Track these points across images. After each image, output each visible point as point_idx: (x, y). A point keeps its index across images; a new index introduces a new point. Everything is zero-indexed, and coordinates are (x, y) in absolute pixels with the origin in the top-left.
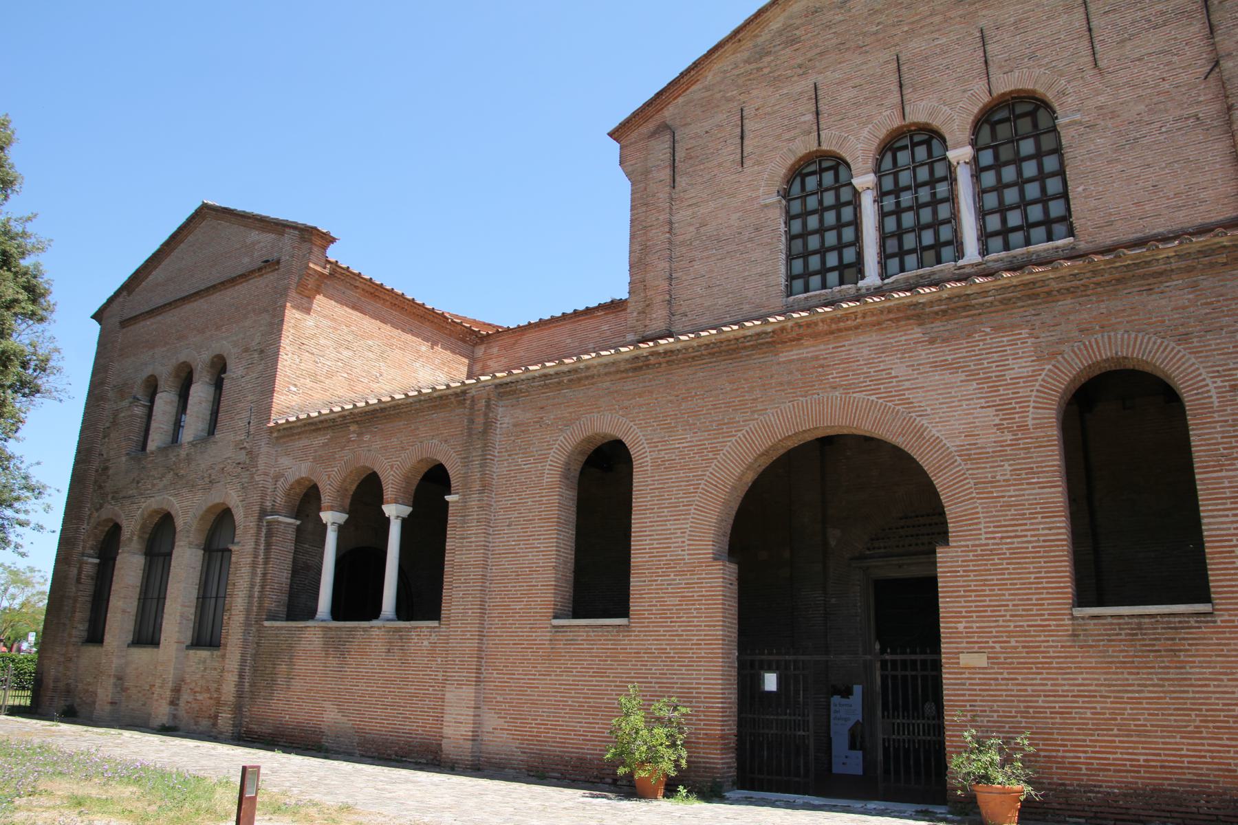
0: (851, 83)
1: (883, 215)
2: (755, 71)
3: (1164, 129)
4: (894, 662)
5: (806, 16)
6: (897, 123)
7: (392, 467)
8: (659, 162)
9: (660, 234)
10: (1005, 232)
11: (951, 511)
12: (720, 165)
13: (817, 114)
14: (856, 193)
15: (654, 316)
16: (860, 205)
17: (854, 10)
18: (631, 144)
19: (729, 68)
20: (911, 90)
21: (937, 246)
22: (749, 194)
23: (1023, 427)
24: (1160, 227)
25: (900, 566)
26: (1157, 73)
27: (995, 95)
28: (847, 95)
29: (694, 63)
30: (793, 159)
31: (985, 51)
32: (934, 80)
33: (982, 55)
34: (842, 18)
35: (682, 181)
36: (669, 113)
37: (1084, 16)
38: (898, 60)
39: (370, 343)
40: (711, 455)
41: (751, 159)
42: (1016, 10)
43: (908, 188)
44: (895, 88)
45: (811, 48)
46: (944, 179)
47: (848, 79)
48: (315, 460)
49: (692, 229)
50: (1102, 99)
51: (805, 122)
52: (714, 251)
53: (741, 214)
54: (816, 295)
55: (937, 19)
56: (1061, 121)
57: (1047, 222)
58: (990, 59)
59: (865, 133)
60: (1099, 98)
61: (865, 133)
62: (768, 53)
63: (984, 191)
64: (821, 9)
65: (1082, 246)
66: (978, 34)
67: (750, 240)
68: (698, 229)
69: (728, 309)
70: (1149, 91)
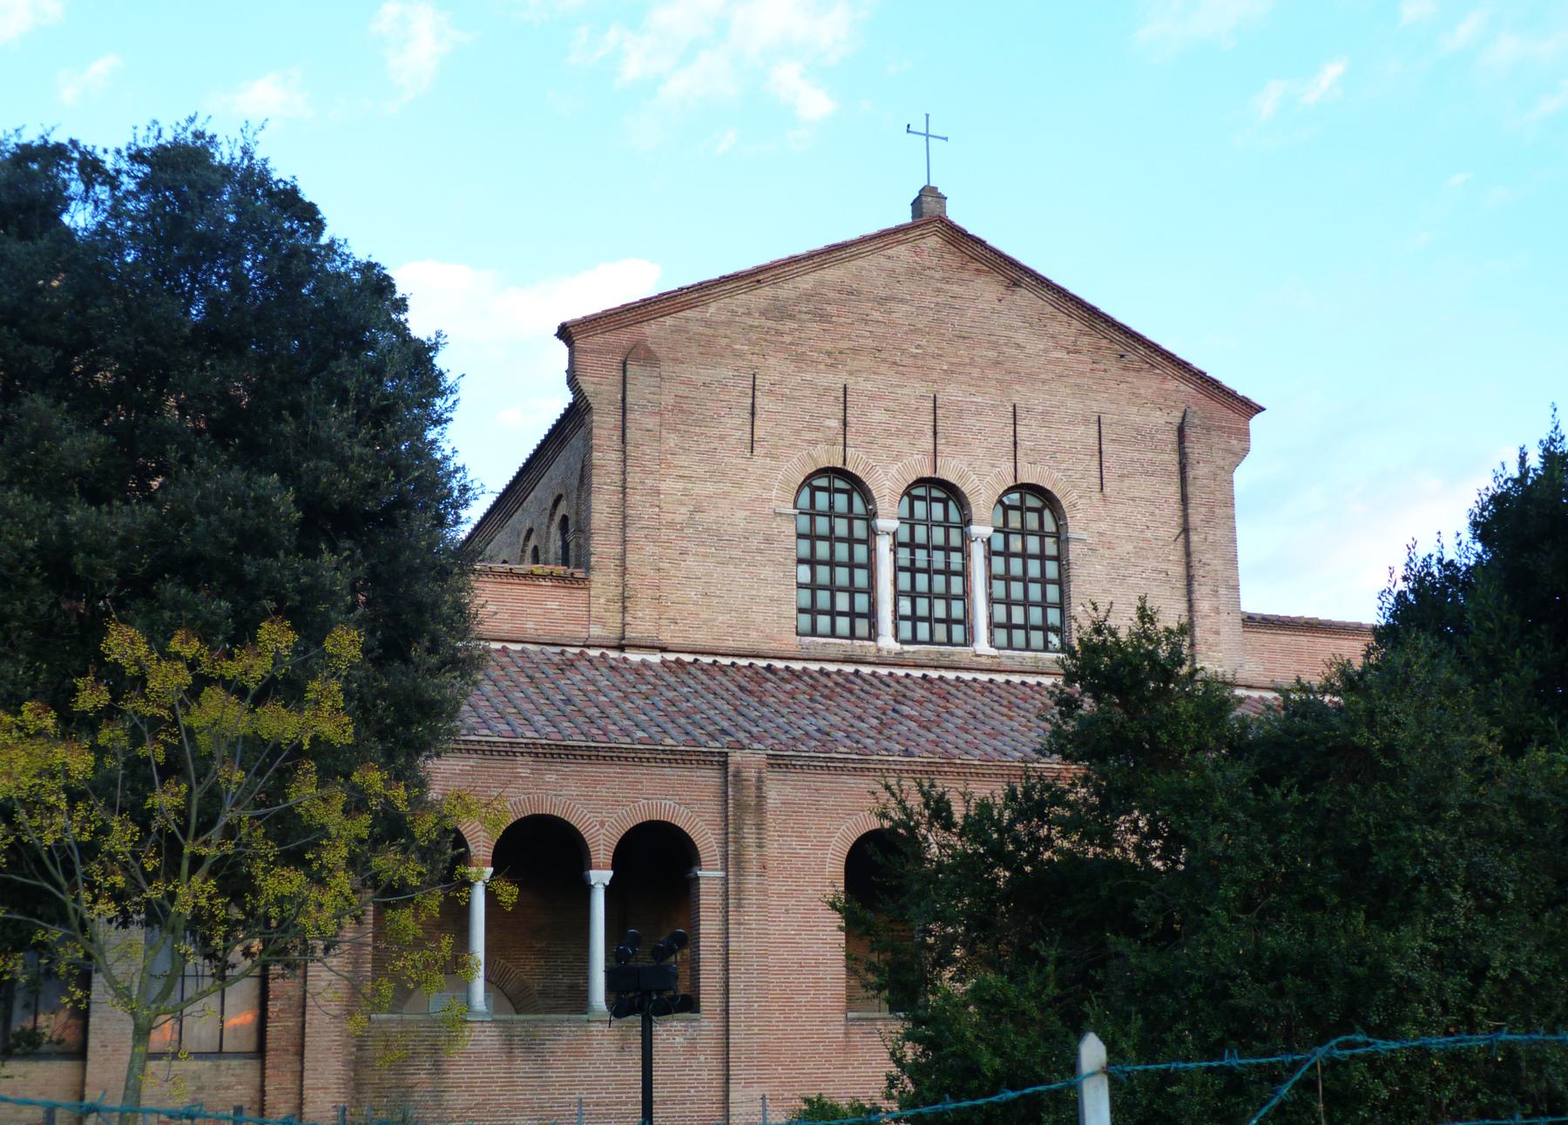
0: (883, 404)
1: (898, 569)
2: (773, 332)
3: (1144, 575)
5: (839, 292)
8: (645, 402)
9: (648, 505)
10: (1009, 626)
12: (722, 438)
13: (845, 424)
14: (872, 532)
15: (640, 614)
16: (875, 550)
17: (894, 315)
18: (593, 351)
19: (740, 311)
20: (943, 441)
21: (949, 621)
22: (759, 492)
26: (1144, 519)
27: (1019, 482)
29: (700, 284)
31: (1015, 430)
32: (967, 441)
33: (1012, 433)
34: (880, 319)
36: (650, 330)
37: (1096, 435)
38: (935, 401)
41: (762, 446)
42: (1044, 399)
44: (931, 433)
45: (843, 338)
47: (881, 397)
49: (683, 510)
50: (1103, 526)
51: (829, 428)
52: (713, 550)
53: (748, 513)
54: (835, 644)
55: (976, 372)
60: (1102, 524)
61: (894, 469)
62: (792, 317)
63: (996, 577)
64: (859, 293)
66: (1011, 409)
67: (760, 551)
68: (691, 512)
69: (731, 630)
70: (1136, 534)
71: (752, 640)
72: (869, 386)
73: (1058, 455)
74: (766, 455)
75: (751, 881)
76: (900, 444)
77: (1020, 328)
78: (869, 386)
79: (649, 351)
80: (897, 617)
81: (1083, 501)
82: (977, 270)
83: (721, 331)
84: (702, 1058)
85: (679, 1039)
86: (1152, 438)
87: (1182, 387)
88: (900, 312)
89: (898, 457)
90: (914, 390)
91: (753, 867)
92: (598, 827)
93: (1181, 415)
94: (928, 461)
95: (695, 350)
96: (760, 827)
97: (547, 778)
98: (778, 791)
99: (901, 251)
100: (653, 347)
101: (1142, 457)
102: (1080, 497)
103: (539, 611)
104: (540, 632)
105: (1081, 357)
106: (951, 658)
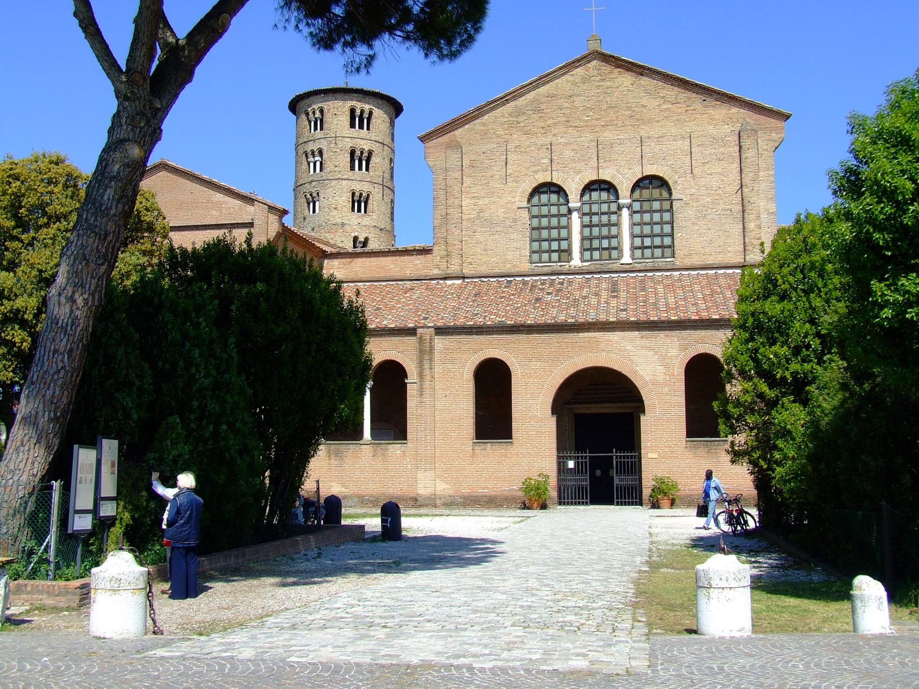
0: (571, 147)
1: (584, 226)
3: (717, 213)
4: (620, 456)
6: (594, 178)
10: (643, 248)
11: (647, 403)
23: (673, 375)
24: (710, 261)
25: (588, 408)
27: (644, 175)
28: (568, 153)
30: (536, 184)
35: (467, 181)
36: (458, 132)
40: (549, 373)
43: (596, 214)
45: (549, 118)
46: (615, 213)
49: (474, 212)
50: (693, 191)
56: (674, 197)
57: (662, 247)
58: (644, 154)
59: (577, 179)
61: (577, 179)
65: (678, 263)
66: (639, 139)
67: (511, 227)
71: (507, 268)
72: (563, 140)
73: (667, 158)
74: (513, 181)
75: (427, 384)
76: (579, 166)
77: (644, 96)
78: (563, 140)
79: (457, 142)
80: (583, 250)
81: (681, 179)
82: (619, 72)
83: (490, 127)
84: (408, 460)
85: (398, 452)
86: (722, 141)
87: (742, 111)
88: (578, 102)
89: (579, 172)
90: (587, 138)
91: (428, 378)
93: (740, 125)
94: (595, 171)
95: (478, 137)
96: (431, 360)
98: (440, 343)
99: (579, 71)
100: (459, 140)
101: (716, 151)
102: (679, 178)
104: (412, 275)
105: (679, 105)
106: (608, 267)
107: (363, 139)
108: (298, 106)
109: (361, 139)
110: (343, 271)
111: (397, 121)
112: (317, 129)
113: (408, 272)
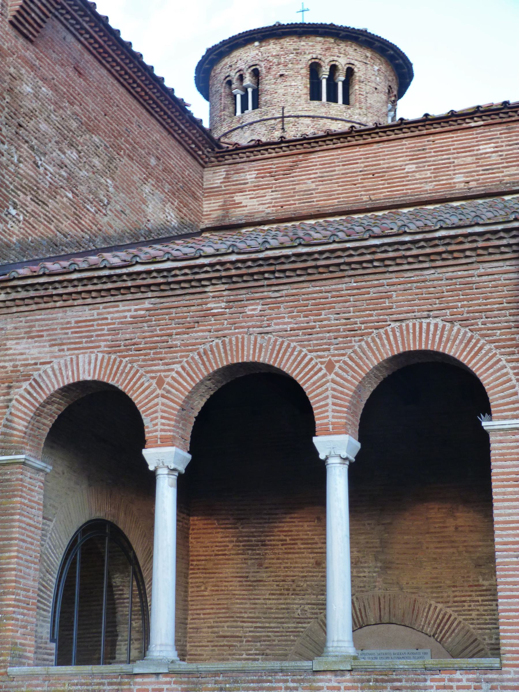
7: (330, 366)
39: (96, 139)
48: (114, 348)
92: (324, 371)
97: (249, 311)
103: (469, 160)
104: (473, 184)
107: (336, 119)
108: (213, 74)
109: (332, 119)
110: (269, 195)
111: (400, 102)
112: (247, 109)
113: (460, 178)
